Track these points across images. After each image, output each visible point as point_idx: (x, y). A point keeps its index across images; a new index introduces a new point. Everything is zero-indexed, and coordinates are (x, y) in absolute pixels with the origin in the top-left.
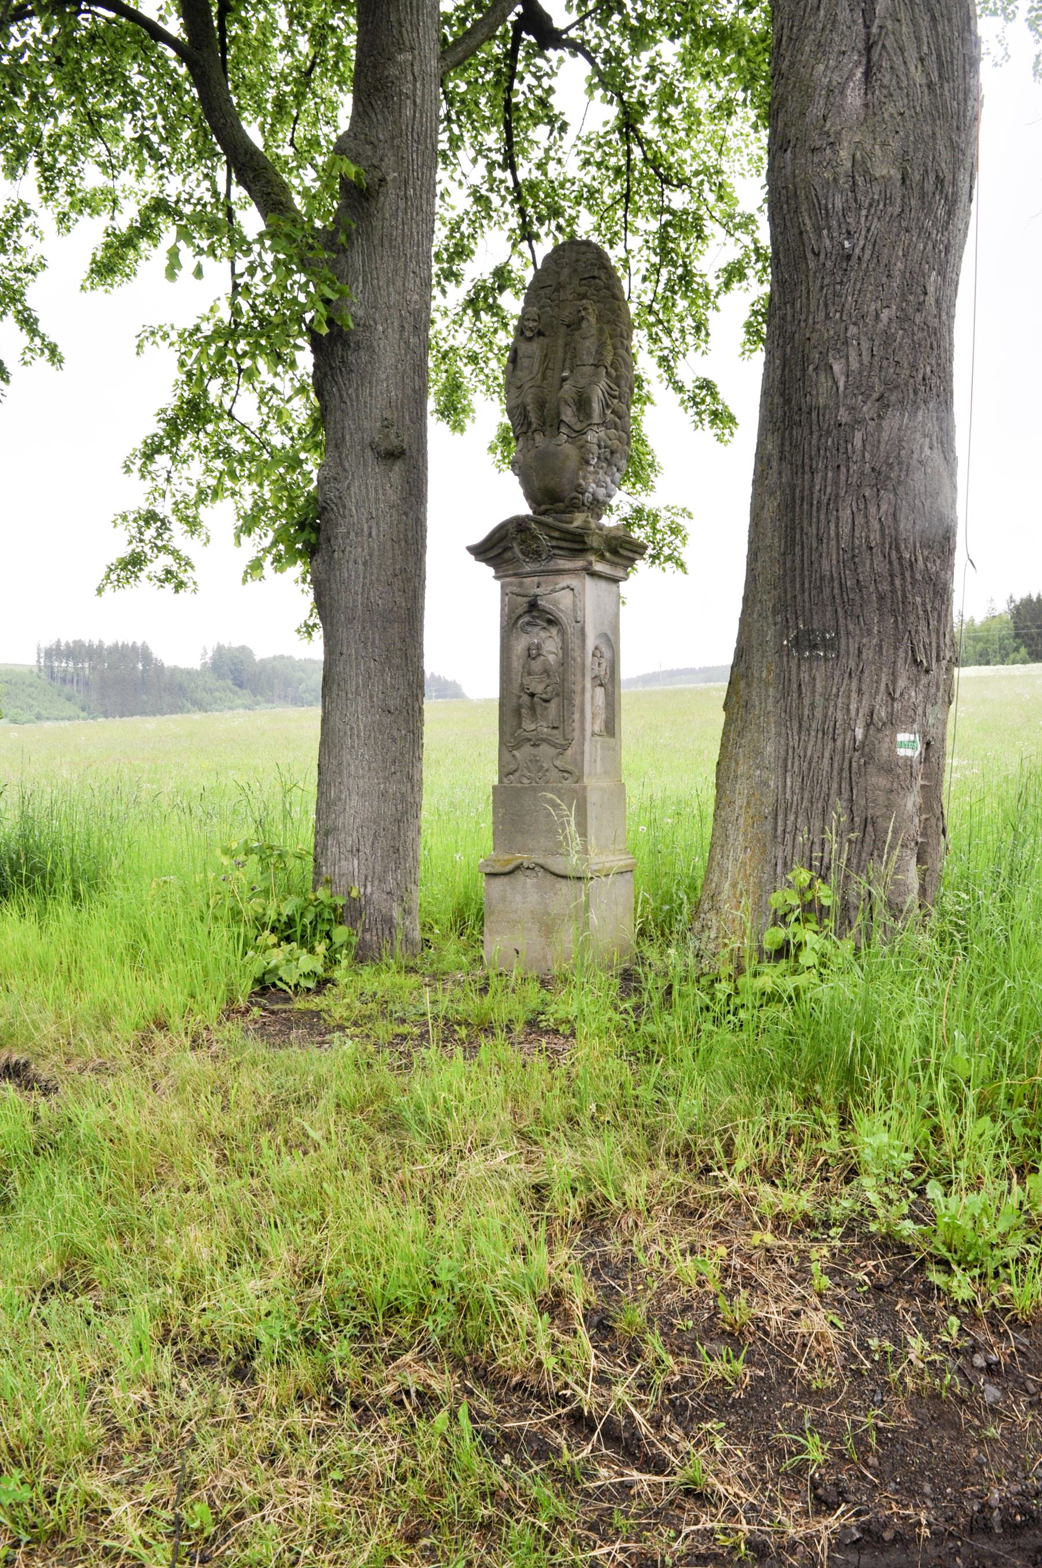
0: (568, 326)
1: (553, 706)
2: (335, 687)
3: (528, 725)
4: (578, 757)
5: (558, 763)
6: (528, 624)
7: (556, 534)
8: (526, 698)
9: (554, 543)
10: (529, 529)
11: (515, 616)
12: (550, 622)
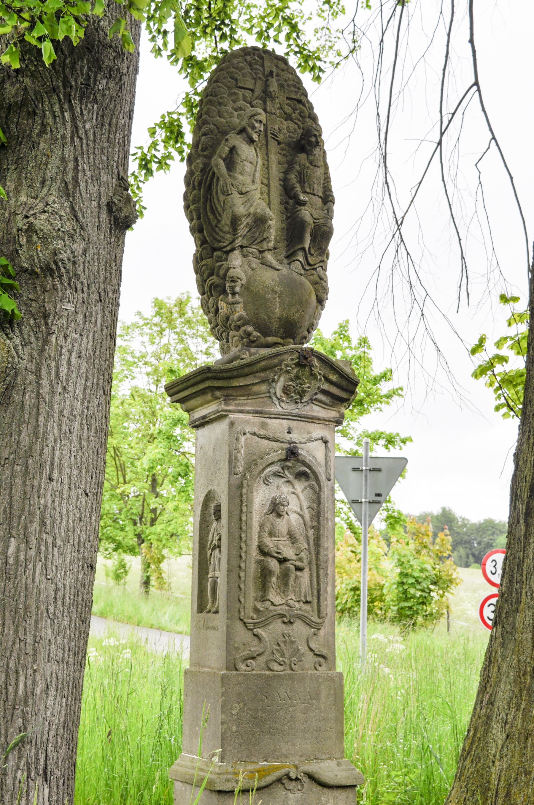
0: (279, 143)
1: (305, 576)
2: (35, 527)
3: (274, 596)
4: (331, 638)
5: (313, 646)
6: (276, 474)
7: (334, 378)
8: (274, 564)
9: (326, 387)
10: (311, 366)
11: (262, 463)
12: (301, 475)
